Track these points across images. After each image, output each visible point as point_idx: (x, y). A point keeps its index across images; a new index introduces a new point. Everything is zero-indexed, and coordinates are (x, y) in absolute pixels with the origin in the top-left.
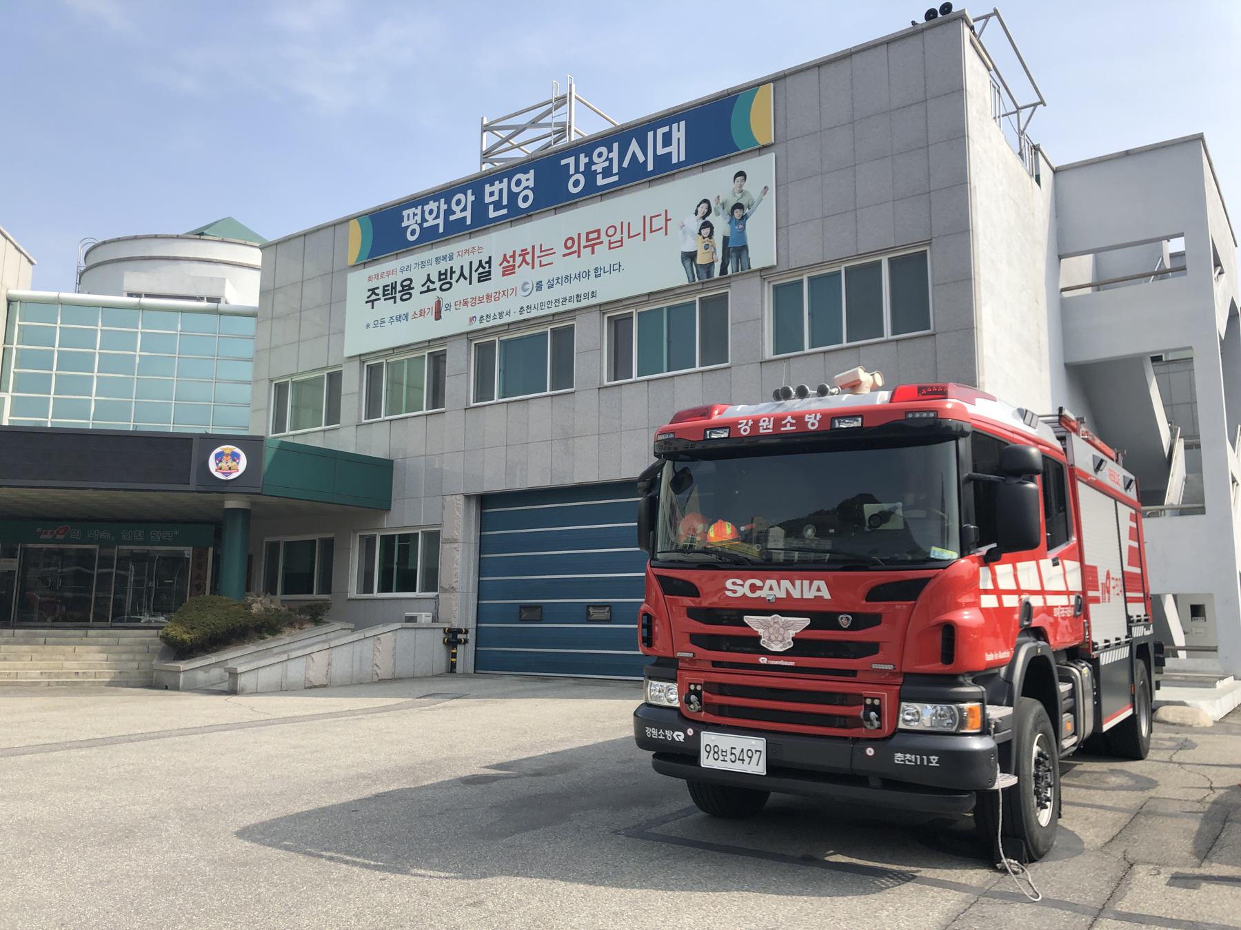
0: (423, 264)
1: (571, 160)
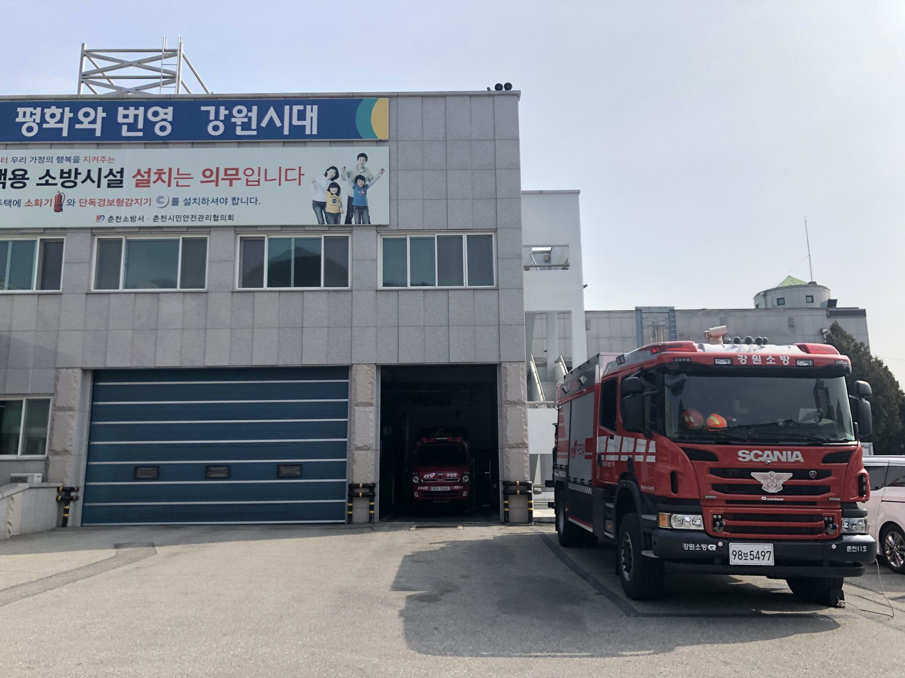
0: (41, 160)
1: (212, 109)
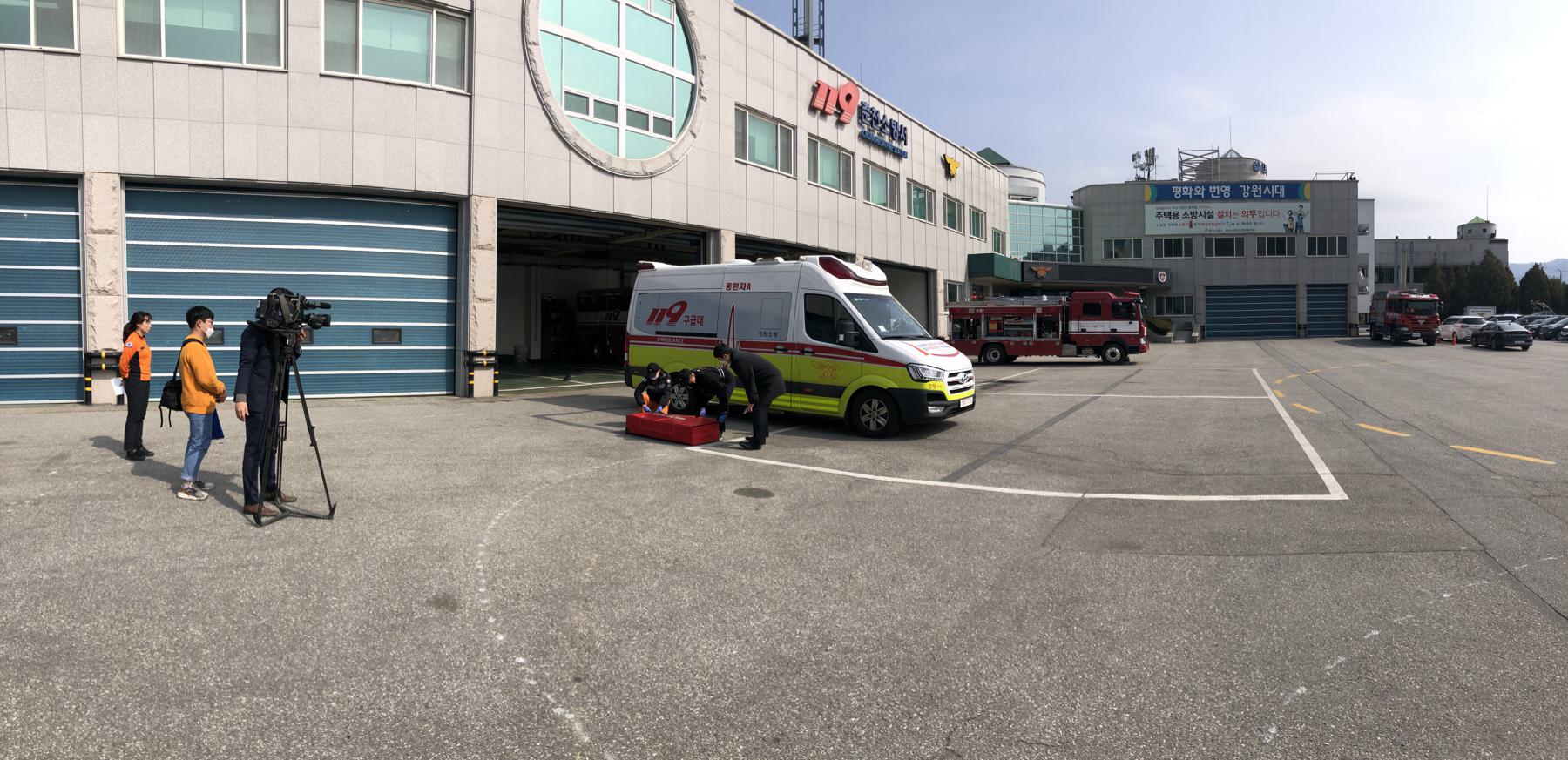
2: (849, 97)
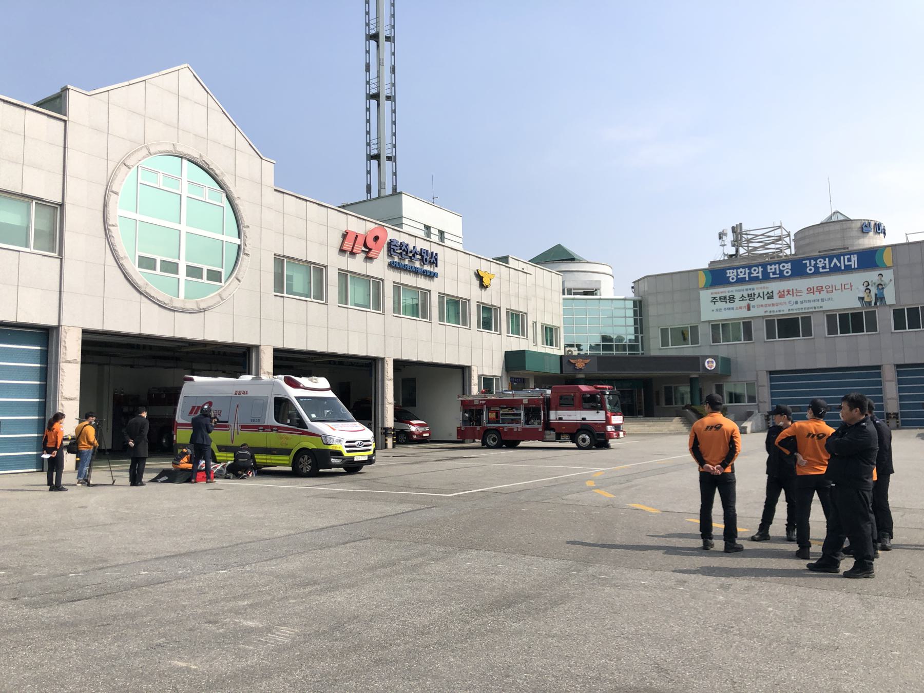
0: (739, 291)
2: (376, 238)
